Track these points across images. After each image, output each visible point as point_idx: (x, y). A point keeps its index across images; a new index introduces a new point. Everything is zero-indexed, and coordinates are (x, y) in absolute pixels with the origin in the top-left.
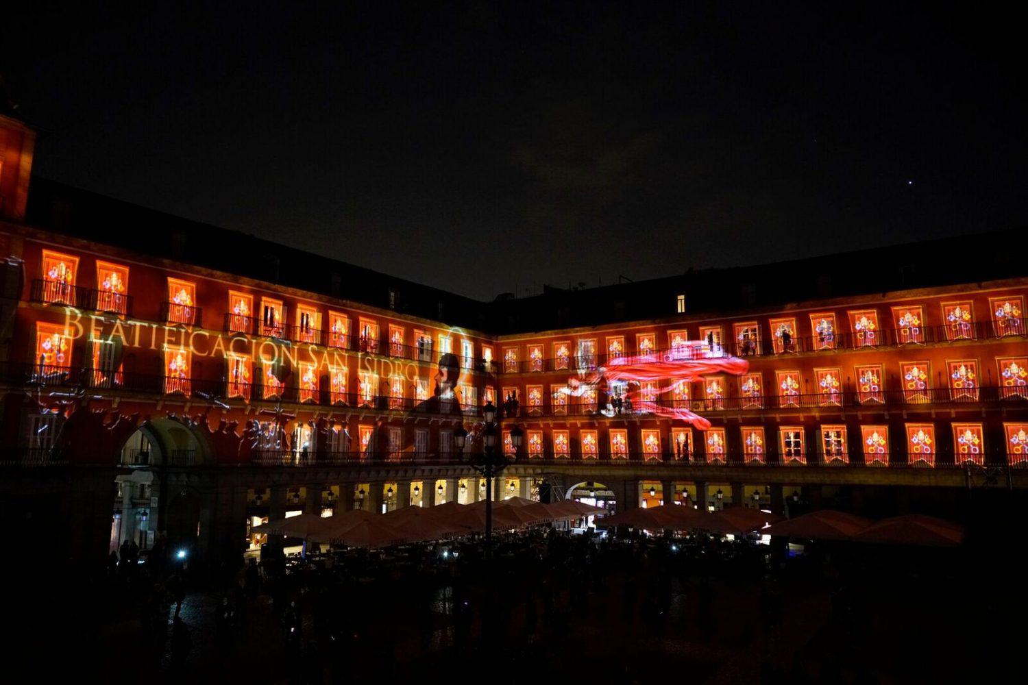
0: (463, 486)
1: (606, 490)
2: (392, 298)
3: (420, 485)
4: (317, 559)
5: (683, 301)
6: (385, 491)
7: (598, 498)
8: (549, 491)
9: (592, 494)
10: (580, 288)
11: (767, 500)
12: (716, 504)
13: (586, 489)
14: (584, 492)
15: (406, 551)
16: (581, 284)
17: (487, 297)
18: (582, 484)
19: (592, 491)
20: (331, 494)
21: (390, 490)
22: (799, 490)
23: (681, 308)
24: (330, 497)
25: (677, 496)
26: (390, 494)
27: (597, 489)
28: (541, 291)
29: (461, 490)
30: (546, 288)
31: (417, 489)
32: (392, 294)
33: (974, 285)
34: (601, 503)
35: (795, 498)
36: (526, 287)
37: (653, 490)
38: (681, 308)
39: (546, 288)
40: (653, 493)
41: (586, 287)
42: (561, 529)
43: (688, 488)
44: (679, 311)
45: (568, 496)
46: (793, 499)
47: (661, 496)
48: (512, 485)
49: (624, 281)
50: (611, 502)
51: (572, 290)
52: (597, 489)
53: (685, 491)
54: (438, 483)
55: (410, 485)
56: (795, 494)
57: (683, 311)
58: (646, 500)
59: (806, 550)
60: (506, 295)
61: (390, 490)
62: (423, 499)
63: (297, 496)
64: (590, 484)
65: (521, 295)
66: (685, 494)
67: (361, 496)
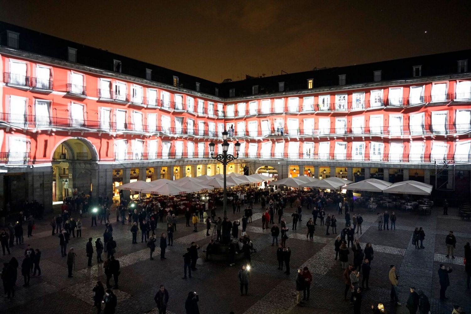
0: (209, 168)
1: (273, 169)
2: (175, 81)
3: (190, 167)
4: (146, 200)
5: (311, 83)
6: (174, 170)
7: (270, 173)
8: (248, 170)
9: (267, 171)
10: (263, 77)
11: (345, 174)
12: (323, 176)
13: (264, 169)
14: (263, 170)
15: (185, 197)
16: (264, 75)
17: (219, 80)
18: (263, 167)
19: (267, 170)
20: (150, 172)
21: (177, 170)
22: (360, 170)
23: (310, 86)
24: (150, 173)
25: (305, 172)
26: (176, 172)
27: (269, 169)
28: (244, 78)
29: (208, 170)
30: (247, 76)
31: (188, 169)
32: (175, 79)
33: (296, 92)
34: (271, 175)
35: (358, 173)
36: (238, 76)
37: (295, 169)
38: (310, 86)
39: (247, 76)
40: (295, 171)
41: (266, 76)
42: (253, 187)
43: (310, 169)
44: (309, 88)
45: (257, 172)
46: (357, 174)
47: (298, 172)
48: (231, 167)
49: (284, 73)
50: (275, 175)
51: (259, 77)
52: (269, 169)
53: (309, 170)
54: (198, 166)
55: (185, 167)
56: (358, 172)
57: (311, 88)
58: (291, 174)
59: (362, 196)
60: (228, 80)
61: (177, 170)
62: (191, 173)
63: (135, 173)
64: (266, 167)
65: (235, 79)
66: (309, 172)
67: (164, 173)
